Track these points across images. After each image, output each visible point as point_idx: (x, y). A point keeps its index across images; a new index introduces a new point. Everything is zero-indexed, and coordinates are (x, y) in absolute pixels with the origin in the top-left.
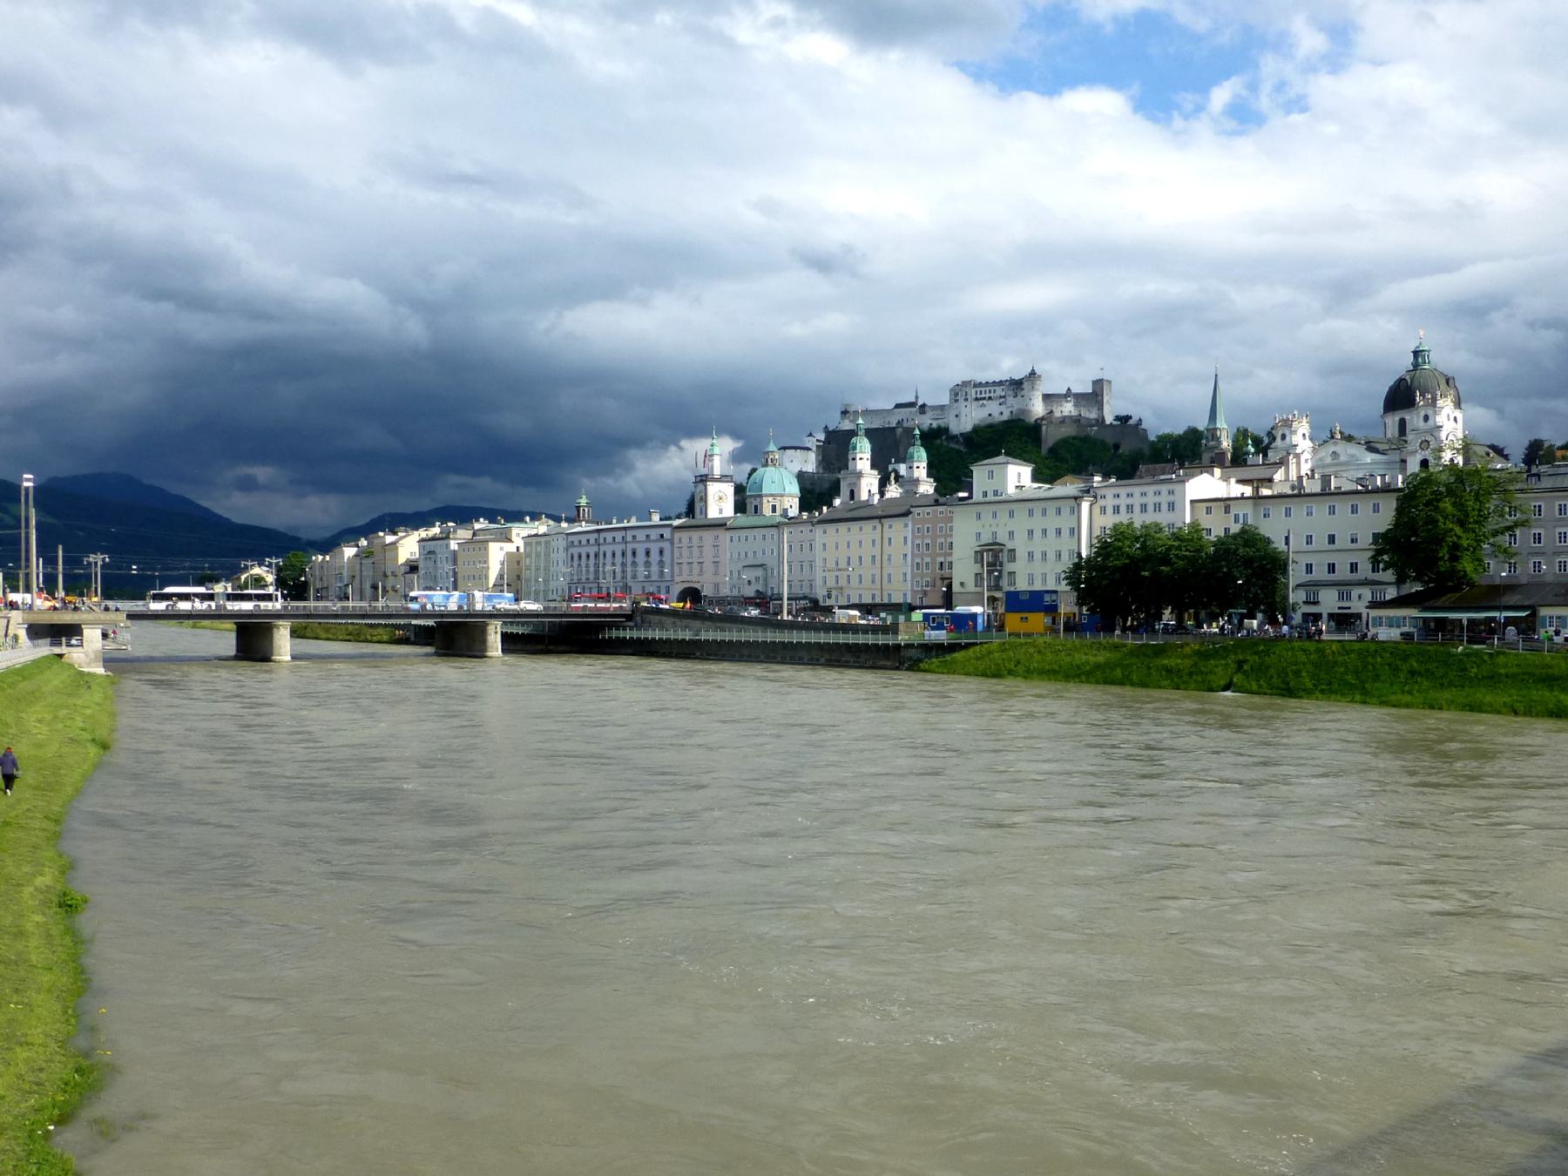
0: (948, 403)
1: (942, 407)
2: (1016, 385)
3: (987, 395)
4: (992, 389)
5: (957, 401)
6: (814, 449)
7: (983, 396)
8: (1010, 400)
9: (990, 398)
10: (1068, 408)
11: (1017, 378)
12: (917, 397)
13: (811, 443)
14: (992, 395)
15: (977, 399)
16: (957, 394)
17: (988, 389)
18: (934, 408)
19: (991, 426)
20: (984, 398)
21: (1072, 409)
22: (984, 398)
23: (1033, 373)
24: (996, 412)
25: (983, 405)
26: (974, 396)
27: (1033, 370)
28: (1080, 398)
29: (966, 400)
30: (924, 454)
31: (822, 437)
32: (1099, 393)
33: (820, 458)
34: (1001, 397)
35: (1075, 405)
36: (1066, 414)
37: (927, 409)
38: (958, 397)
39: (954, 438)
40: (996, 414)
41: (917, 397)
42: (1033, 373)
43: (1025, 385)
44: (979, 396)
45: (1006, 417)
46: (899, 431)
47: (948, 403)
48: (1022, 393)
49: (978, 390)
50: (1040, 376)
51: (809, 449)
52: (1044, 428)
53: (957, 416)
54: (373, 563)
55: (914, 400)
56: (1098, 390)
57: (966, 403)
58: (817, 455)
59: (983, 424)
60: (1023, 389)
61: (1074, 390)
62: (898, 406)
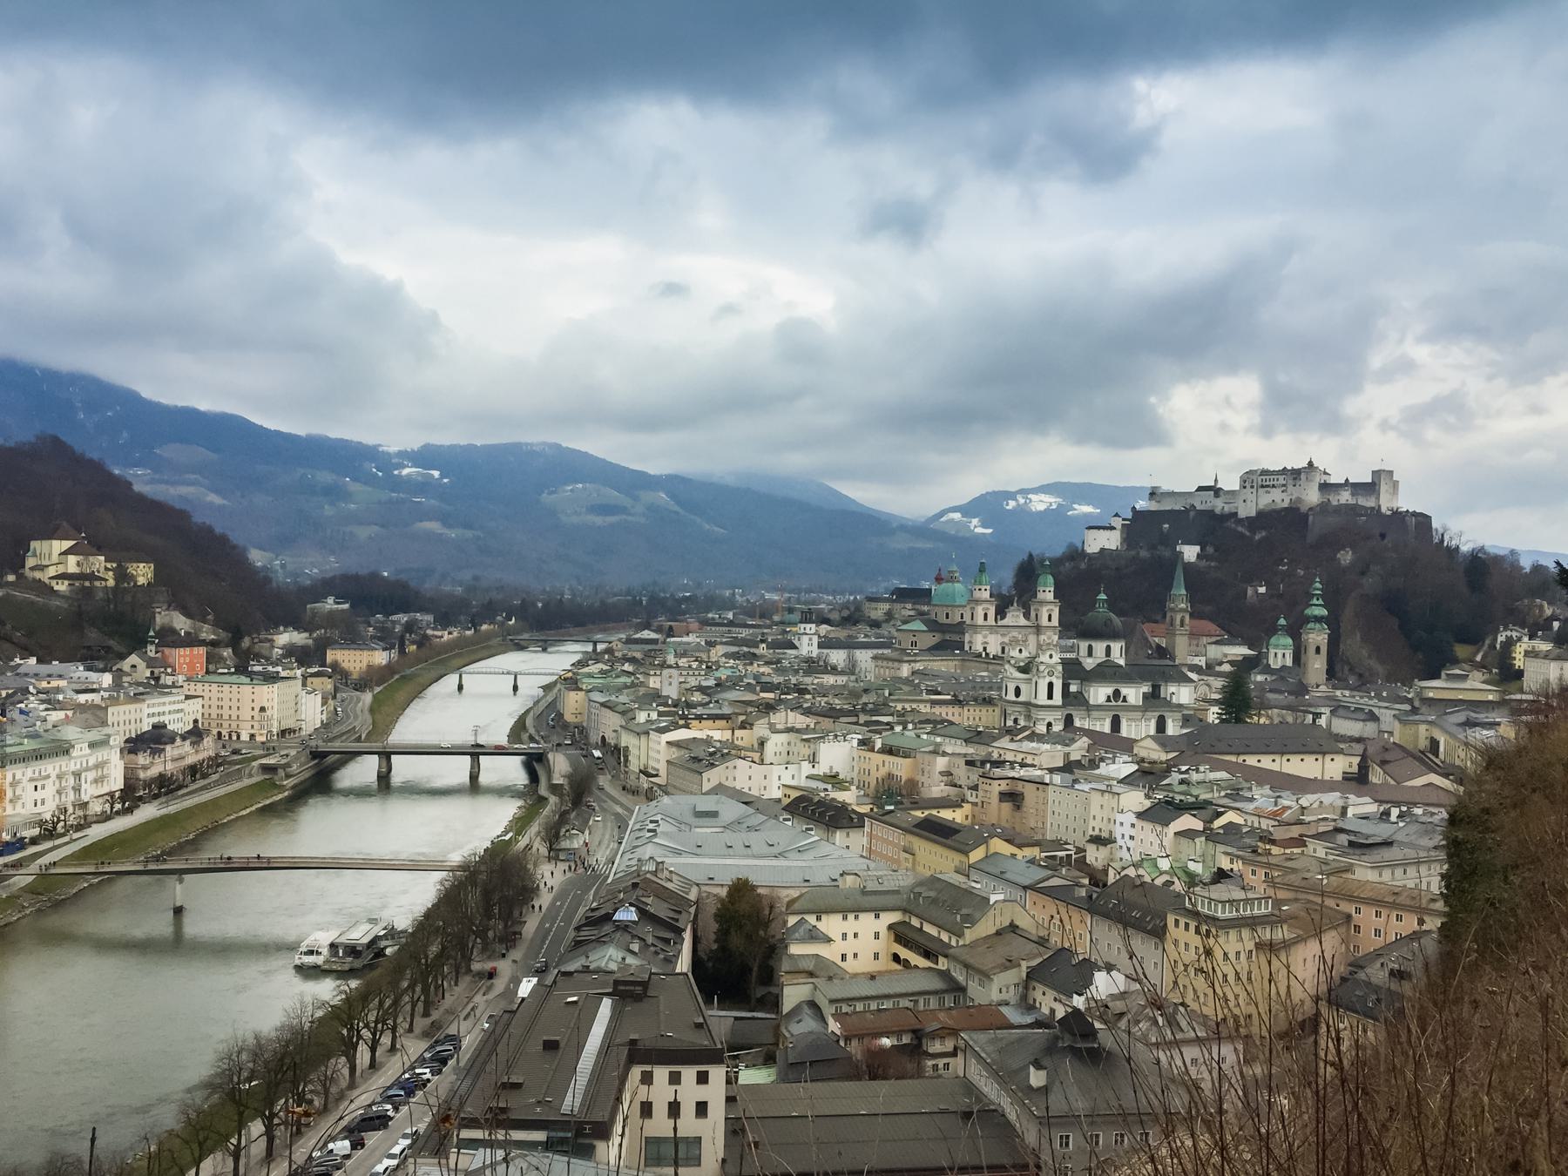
0: (1238, 488)
1: (1234, 492)
2: (1295, 474)
3: (1272, 483)
4: (1276, 477)
5: (1245, 487)
6: (1119, 527)
7: (1268, 483)
8: (1290, 487)
9: (1274, 486)
10: (1345, 497)
12: (1216, 480)
13: (1118, 522)
14: (1275, 483)
15: (1262, 486)
16: (1245, 482)
18: (1228, 492)
19: (1275, 511)
20: (1268, 486)
21: (1350, 498)
22: (1268, 486)
23: (1310, 464)
24: (1278, 498)
25: (1268, 492)
26: (1260, 483)
28: (1358, 488)
29: (1252, 487)
30: (1050, 579)
31: (1130, 516)
32: (1377, 482)
33: (1125, 536)
34: (1284, 485)
35: (1353, 494)
36: (1343, 501)
37: (1221, 493)
39: (1240, 521)
40: (1278, 500)
41: (1216, 480)
42: (1310, 464)
43: (1303, 476)
44: (1264, 484)
45: (1286, 505)
46: (1192, 514)
47: (1238, 488)
49: (1264, 478)
51: (1112, 528)
52: (1311, 518)
58: (1122, 533)
59: (1267, 509)
62: (1200, 489)
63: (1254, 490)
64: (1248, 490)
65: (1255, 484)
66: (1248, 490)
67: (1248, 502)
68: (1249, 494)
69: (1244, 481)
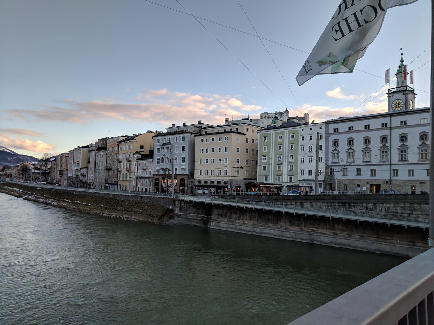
1: (257, 120)
7: (271, 117)
11: (281, 112)
12: (249, 117)
15: (268, 118)
17: (272, 115)
18: (255, 120)
20: (271, 118)
22: (271, 118)
23: (287, 110)
27: (287, 109)
28: (300, 119)
29: (265, 118)
35: (299, 121)
38: (263, 117)
41: (249, 117)
42: (287, 110)
43: (285, 114)
48: (283, 116)
50: (289, 111)
53: (262, 123)
54: (107, 154)
55: (248, 118)
56: (305, 117)
57: (265, 119)
60: (283, 115)
61: (298, 117)
62: (242, 120)
63: (266, 119)
64: (264, 119)
65: (266, 117)
66: (264, 119)
67: (264, 123)
68: (263, 120)
69: (262, 116)
